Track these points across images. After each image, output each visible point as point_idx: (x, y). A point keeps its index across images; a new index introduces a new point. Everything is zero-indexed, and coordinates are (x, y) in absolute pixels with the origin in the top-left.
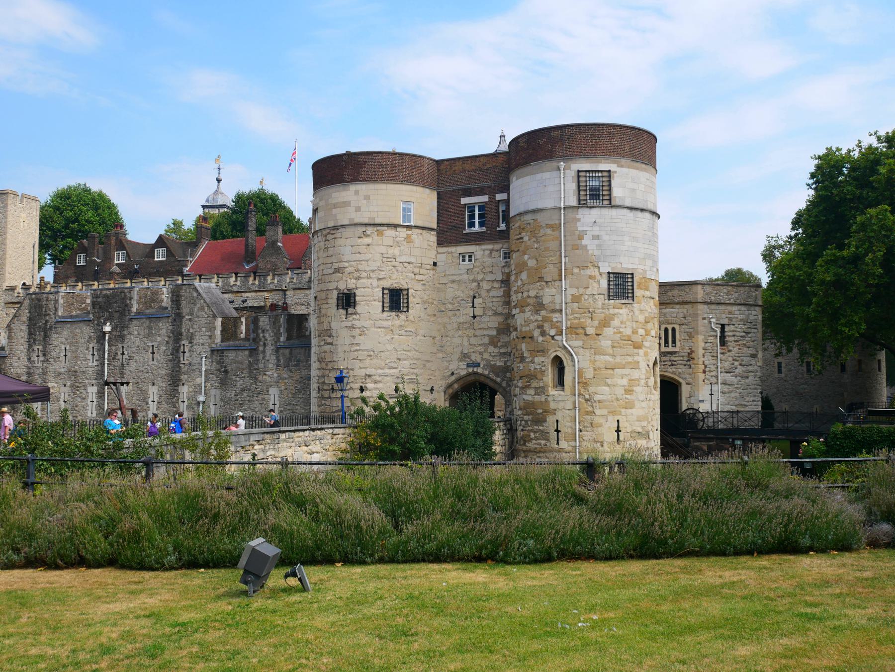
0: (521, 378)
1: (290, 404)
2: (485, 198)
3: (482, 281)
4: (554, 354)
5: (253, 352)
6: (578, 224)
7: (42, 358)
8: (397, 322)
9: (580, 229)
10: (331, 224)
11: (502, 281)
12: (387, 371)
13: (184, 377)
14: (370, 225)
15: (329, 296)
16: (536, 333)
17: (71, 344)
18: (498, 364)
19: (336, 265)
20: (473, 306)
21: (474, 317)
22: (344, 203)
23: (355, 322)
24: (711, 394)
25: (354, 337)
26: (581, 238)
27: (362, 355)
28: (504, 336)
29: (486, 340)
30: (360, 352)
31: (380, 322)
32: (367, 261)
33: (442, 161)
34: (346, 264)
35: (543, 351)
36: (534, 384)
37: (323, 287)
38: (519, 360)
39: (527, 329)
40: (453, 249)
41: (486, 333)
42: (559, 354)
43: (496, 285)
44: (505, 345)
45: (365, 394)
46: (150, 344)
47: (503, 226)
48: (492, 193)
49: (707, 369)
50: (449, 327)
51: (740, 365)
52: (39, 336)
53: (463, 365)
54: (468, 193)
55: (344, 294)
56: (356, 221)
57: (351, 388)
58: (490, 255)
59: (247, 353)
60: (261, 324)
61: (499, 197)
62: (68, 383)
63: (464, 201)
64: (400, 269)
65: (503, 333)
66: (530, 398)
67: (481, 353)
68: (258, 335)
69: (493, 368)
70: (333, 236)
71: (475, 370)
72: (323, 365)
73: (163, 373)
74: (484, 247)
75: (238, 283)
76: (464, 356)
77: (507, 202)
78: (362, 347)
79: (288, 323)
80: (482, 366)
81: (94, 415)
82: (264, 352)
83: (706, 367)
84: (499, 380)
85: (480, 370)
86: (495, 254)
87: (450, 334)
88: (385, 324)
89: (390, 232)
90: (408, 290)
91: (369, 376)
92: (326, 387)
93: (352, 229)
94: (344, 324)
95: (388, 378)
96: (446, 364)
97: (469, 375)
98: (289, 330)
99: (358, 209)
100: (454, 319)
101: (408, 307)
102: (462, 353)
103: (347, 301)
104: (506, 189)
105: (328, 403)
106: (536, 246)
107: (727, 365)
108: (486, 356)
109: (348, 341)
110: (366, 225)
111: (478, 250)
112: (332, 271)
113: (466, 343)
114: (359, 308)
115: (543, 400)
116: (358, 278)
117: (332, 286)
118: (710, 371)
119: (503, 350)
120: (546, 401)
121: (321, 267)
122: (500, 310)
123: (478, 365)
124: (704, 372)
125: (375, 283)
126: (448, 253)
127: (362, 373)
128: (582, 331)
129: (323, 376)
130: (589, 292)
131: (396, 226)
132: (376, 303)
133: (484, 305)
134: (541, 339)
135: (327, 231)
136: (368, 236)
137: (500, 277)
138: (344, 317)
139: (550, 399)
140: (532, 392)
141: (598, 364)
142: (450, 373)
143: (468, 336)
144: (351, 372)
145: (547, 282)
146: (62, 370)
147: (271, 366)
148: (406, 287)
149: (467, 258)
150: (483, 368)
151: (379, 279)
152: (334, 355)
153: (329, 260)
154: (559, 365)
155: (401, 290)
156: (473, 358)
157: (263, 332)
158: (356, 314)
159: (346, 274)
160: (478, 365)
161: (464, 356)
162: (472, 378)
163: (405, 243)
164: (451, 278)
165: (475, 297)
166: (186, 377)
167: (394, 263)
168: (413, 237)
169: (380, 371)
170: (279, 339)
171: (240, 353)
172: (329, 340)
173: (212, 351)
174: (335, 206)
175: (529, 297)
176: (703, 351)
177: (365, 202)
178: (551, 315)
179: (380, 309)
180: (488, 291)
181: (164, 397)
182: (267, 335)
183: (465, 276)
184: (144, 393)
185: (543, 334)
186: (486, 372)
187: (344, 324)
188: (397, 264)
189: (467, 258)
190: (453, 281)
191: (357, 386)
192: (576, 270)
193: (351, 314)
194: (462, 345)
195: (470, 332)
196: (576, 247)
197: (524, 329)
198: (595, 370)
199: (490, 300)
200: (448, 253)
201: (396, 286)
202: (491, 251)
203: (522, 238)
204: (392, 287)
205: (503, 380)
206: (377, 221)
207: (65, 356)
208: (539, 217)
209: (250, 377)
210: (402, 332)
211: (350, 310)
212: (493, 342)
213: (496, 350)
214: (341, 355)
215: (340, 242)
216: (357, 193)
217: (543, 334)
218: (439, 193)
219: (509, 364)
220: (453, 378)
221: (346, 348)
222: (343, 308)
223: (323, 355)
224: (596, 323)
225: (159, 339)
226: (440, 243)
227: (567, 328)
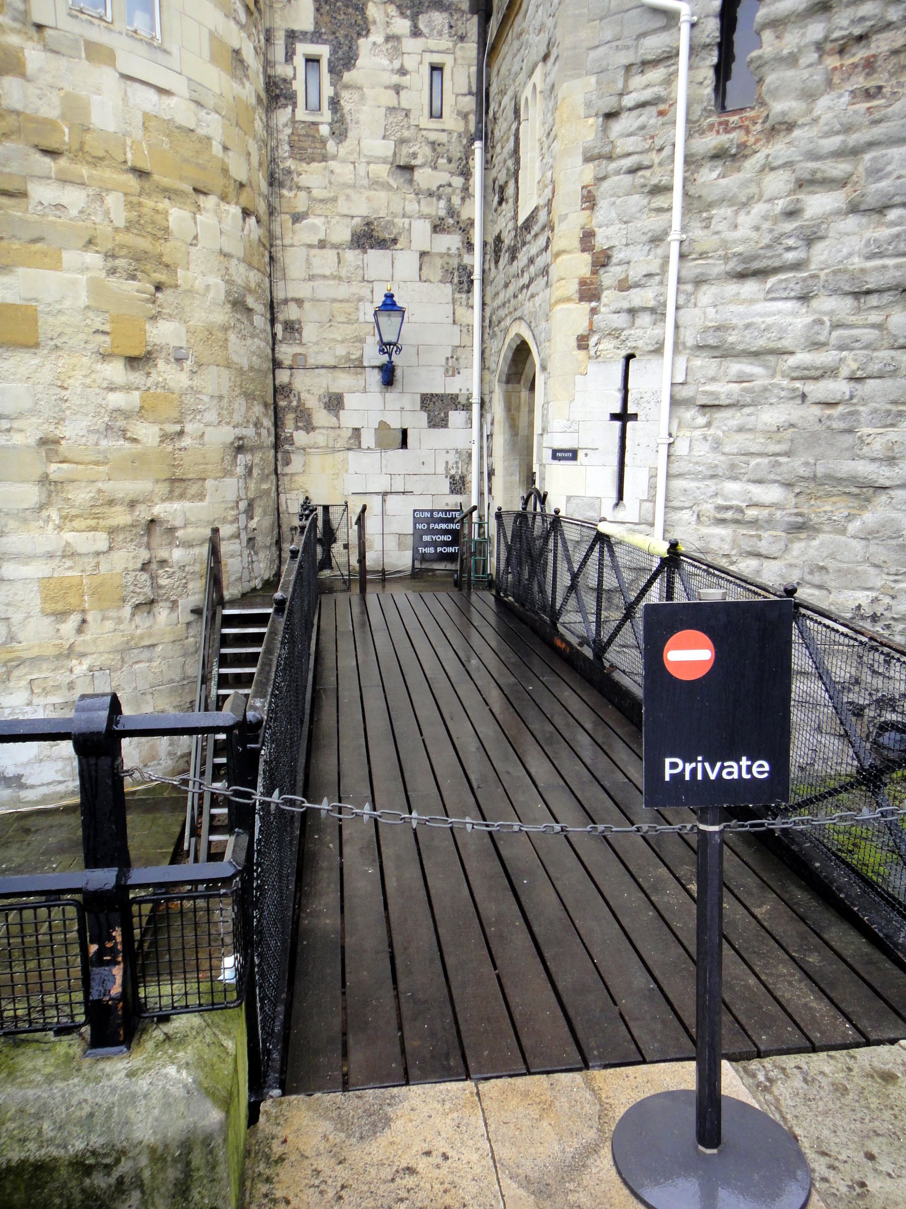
24: (623, 417)
49: (609, 277)
51: (854, 209)
83: (602, 261)
107: (744, 230)
118: (624, 286)
124: (589, 292)
176: (588, 172)
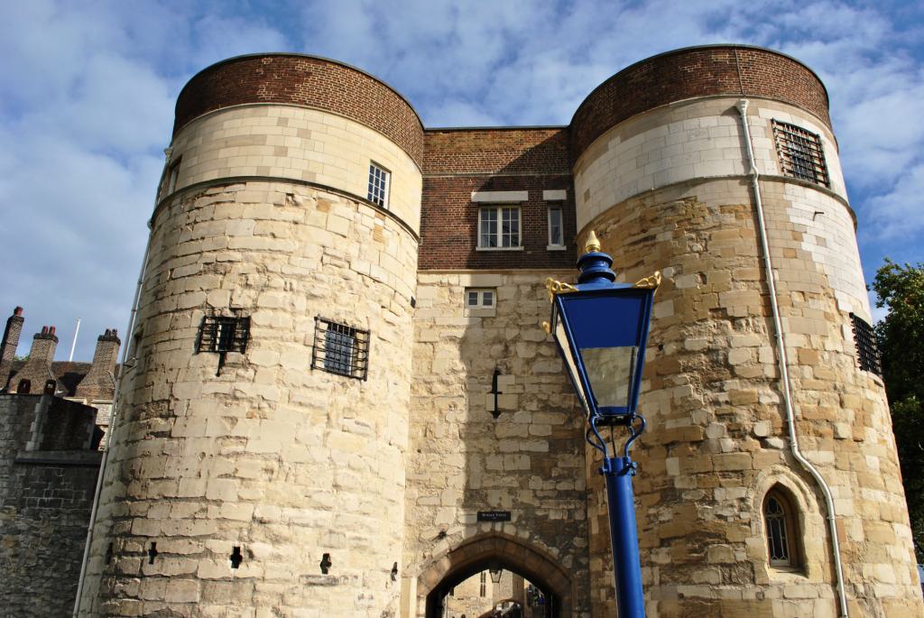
0: (664, 542)
1: (18, 591)
2: (522, 196)
3: (515, 340)
4: (770, 481)
6: (789, 211)
8: (342, 400)
9: (793, 220)
12: (309, 515)
14: (305, 183)
15: (181, 324)
16: (716, 431)
18: (553, 516)
19: (211, 257)
20: (495, 391)
21: (496, 413)
22: (252, 137)
23: (244, 387)
25: (234, 420)
26: (797, 236)
28: (567, 456)
29: (525, 463)
30: (244, 460)
31: (309, 393)
32: (289, 254)
33: (436, 131)
34: (237, 256)
35: (740, 473)
36: (720, 553)
38: (657, 497)
39: (685, 422)
41: (524, 447)
42: (784, 480)
44: (570, 475)
45: (243, 570)
50: (440, 431)
55: (222, 319)
57: (209, 553)
58: (531, 296)
61: (549, 195)
64: (356, 286)
65: (565, 450)
66: (706, 593)
67: (511, 491)
69: (543, 527)
70: (213, 200)
71: (498, 527)
78: (252, 447)
79: (49, 413)
80: (514, 519)
84: (555, 551)
85: (509, 530)
89: (342, 207)
90: (367, 333)
91: (262, 522)
94: (211, 388)
95: (308, 531)
96: (428, 512)
97: (481, 538)
98: (49, 429)
101: (365, 369)
103: (229, 334)
105: (131, 590)
106: (699, 247)
108: (526, 497)
109: (214, 430)
114: (254, 354)
115: (751, 592)
116: (265, 287)
119: (563, 486)
120: (761, 598)
122: (556, 399)
123: (505, 517)
125: (301, 303)
126: (441, 284)
127: (244, 513)
128: (825, 429)
130: (830, 346)
131: (357, 200)
132: (299, 346)
133: (520, 390)
134: (730, 443)
136: (297, 204)
138: (212, 371)
139: (772, 594)
140: (714, 575)
141: (871, 511)
142: (436, 533)
143: (481, 452)
144: (213, 508)
145: (733, 319)
148: (365, 327)
149: (480, 298)
150: (516, 525)
151: (312, 297)
152: (173, 463)
154: (781, 507)
155: (353, 331)
156: (493, 501)
158: (247, 365)
159: (234, 276)
160: (505, 517)
163: (370, 238)
165: (497, 373)
167: (346, 271)
168: (385, 233)
169: (290, 512)
170: (24, 444)
172: (161, 424)
175: (683, 352)
177: (298, 141)
178: (755, 390)
179: (309, 361)
180: (529, 362)
185: (737, 432)
186: (526, 535)
187: (211, 388)
188: (353, 275)
189: (480, 298)
191: (225, 547)
192: (797, 298)
193: (234, 365)
196: (792, 253)
197: (670, 425)
198: (865, 522)
199: (535, 379)
200: (441, 284)
203: (653, 237)
204: (339, 319)
205: (564, 552)
208: (697, 192)
210: (349, 424)
211: (232, 357)
212: (540, 466)
213: (548, 485)
214: (192, 463)
217: (737, 432)
218: (425, 181)
219: (579, 516)
220: (444, 546)
221: (209, 447)
222: (212, 350)
224: (850, 414)
226: (424, 266)
227: (796, 419)
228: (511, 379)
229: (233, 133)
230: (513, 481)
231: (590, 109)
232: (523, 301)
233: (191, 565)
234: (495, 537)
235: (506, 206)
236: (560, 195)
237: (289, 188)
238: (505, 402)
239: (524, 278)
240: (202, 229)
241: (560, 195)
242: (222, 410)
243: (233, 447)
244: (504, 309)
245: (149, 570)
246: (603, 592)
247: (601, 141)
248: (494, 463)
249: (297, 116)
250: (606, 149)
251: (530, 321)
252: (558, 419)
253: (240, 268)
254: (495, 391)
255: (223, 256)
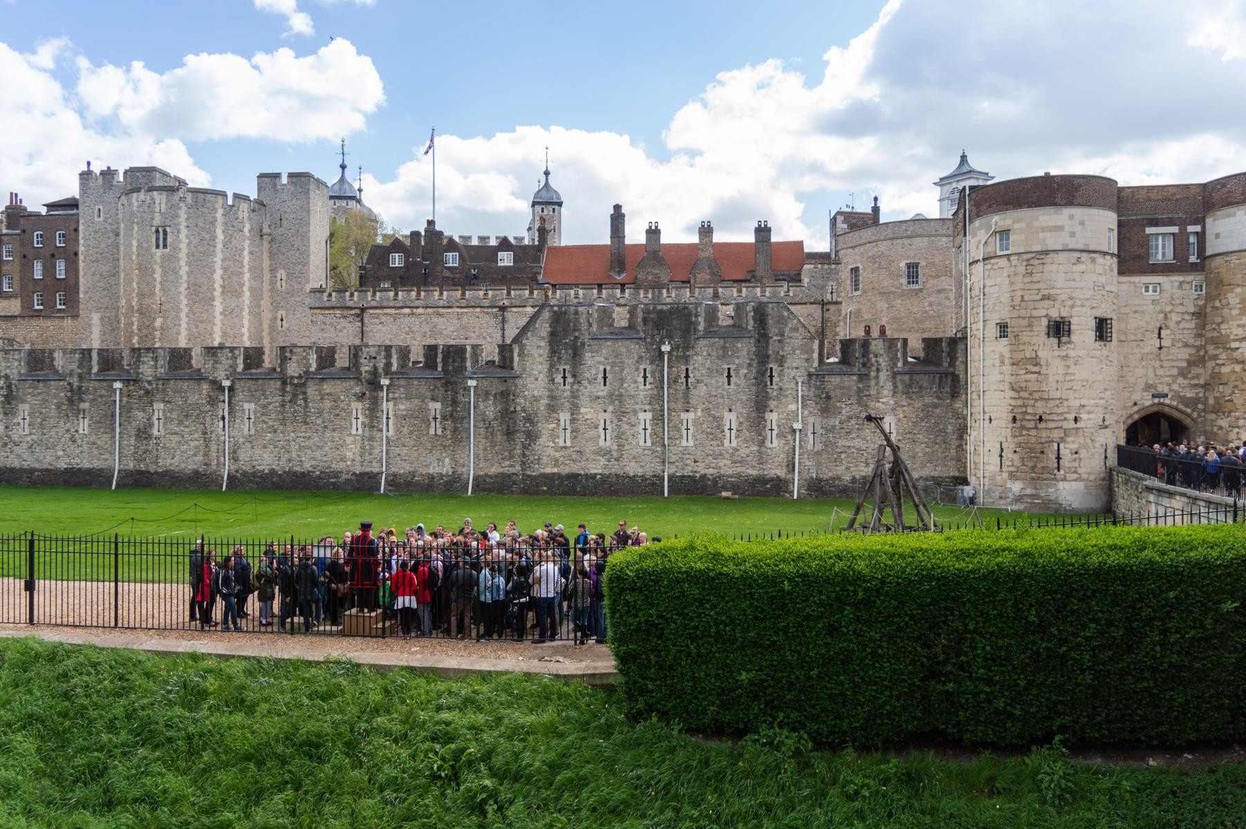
2: (1175, 229)
5: (863, 377)
7: (570, 380)
8: (1105, 352)
10: (1039, 248)
11: (1193, 314)
13: (772, 404)
15: (1035, 323)
17: (613, 365)
18: (1188, 395)
19: (1046, 292)
20: (1159, 337)
21: (1160, 348)
23: (1072, 353)
25: (1068, 367)
27: (1076, 386)
29: (1175, 372)
34: (1059, 291)
37: (1023, 313)
40: (1136, 279)
41: (1175, 364)
43: (1187, 317)
45: (1079, 425)
46: (726, 366)
47: (1193, 259)
48: (1183, 224)
52: (566, 354)
53: (1148, 396)
54: (1155, 223)
56: (1070, 247)
57: (1065, 419)
59: (855, 378)
60: (872, 348)
61: (1191, 229)
62: (611, 408)
63: (1149, 230)
67: (1169, 385)
68: (869, 360)
69: (1183, 400)
72: (1022, 394)
73: (744, 398)
74: (1172, 278)
75: (627, 295)
76: (1148, 387)
77: (1201, 236)
78: (1077, 377)
81: (649, 443)
82: (877, 377)
84: (1189, 411)
85: (1167, 401)
86: (1184, 286)
87: (1132, 364)
88: (1098, 353)
92: (1028, 417)
93: (1066, 255)
94: (1057, 353)
97: (1152, 406)
99: (1073, 235)
100: (1137, 350)
102: (1146, 383)
103: (1059, 329)
104: (1201, 221)
108: (1175, 387)
110: (1082, 251)
111: (1169, 282)
112: (1039, 297)
113: (1151, 374)
116: (1072, 307)
117: (1035, 313)
121: (1020, 293)
122: (1191, 341)
123: (1166, 396)
127: (1077, 403)
129: (1024, 406)
131: (1105, 253)
135: (1029, 256)
137: (1192, 310)
138: (1056, 346)
146: (600, 394)
147: (885, 393)
149: (1151, 288)
153: (1036, 286)
156: (1160, 388)
157: (876, 356)
158: (1070, 342)
160: (1166, 396)
161: (1148, 387)
162: (1155, 409)
164: (1134, 309)
165: (1160, 329)
166: (775, 403)
170: (895, 364)
171: (846, 378)
172: (1036, 369)
173: (810, 375)
174: (1043, 230)
180: (1178, 323)
181: (746, 424)
182: (881, 360)
183: (1151, 307)
184: (718, 420)
186: (1175, 403)
190: (1136, 312)
191: (1072, 416)
194: (1146, 376)
195: (1157, 364)
201: (1104, 315)
202: (1181, 283)
205: (1194, 411)
206: (1092, 247)
207: (605, 378)
209: (859, 403)
211: (1064, 339)
212: (1183, 373)
213: (1186, 382)
215: (1048, 268)
216: (1071, 217)
219: (1201, 395)
220: (1136, 408)
221: (1060, 378)
223: (1023, 385)
225: (737, 361)
226: (1120, 273)
228: (1168, 332)
229: (1043, 224)
230: (1169, 380)
231: (1224, 186)
232: (1175, 291)
233: (1060, 424)
234: (1160, 404)
235: (1164, 235)
236: (1198, 228)
237: (1077, 255)
238: (1165, 343)
239: (1177, 278)
240: (1037, 277)
241: (1198, 228)
242: (1063, 363)
243: (1068, 378)
244: (1164, 295)
245: (1040, 426)
246: (1215, 429)
247: (1232, 210)
248: (1160, 372)
249: (1078, 212)
250: (1234, 215)
251: (1178, 302)
252: (1193, 351)
253: (1064, 297)
254: (1159, 337)
255: (1052, 292)
